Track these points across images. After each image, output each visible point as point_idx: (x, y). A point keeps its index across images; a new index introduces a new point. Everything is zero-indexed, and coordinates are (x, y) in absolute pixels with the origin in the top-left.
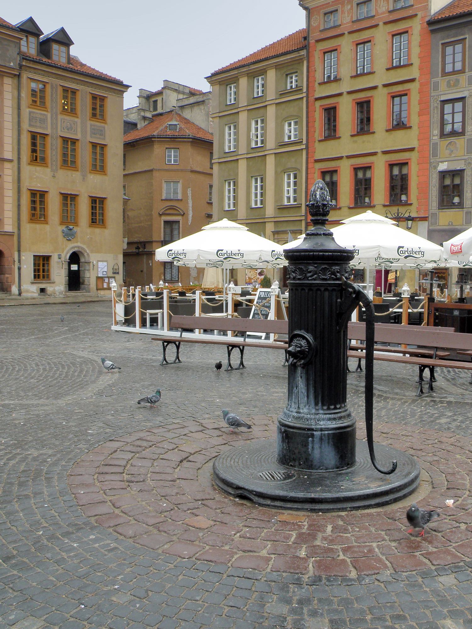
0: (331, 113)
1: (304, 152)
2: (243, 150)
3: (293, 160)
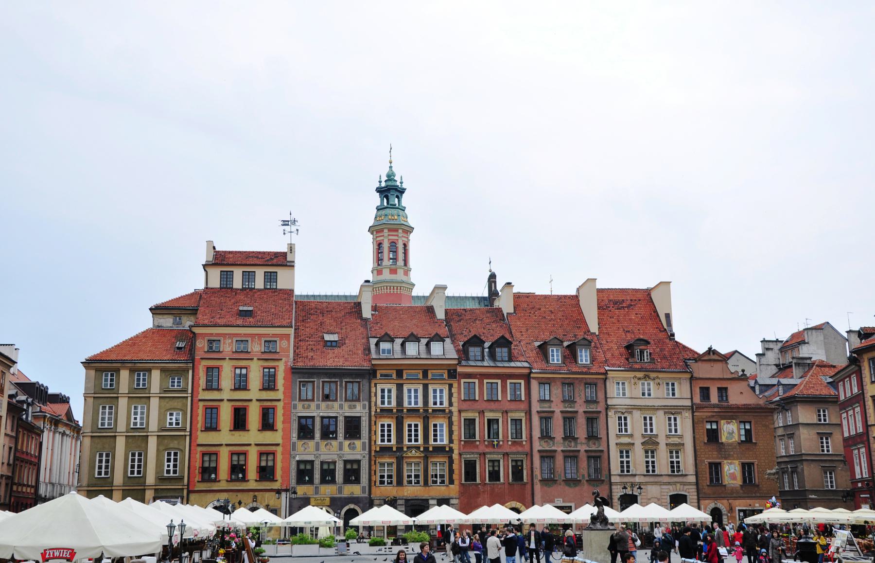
0: (212, 411)
1: (188, 438)
3: (176, 442)
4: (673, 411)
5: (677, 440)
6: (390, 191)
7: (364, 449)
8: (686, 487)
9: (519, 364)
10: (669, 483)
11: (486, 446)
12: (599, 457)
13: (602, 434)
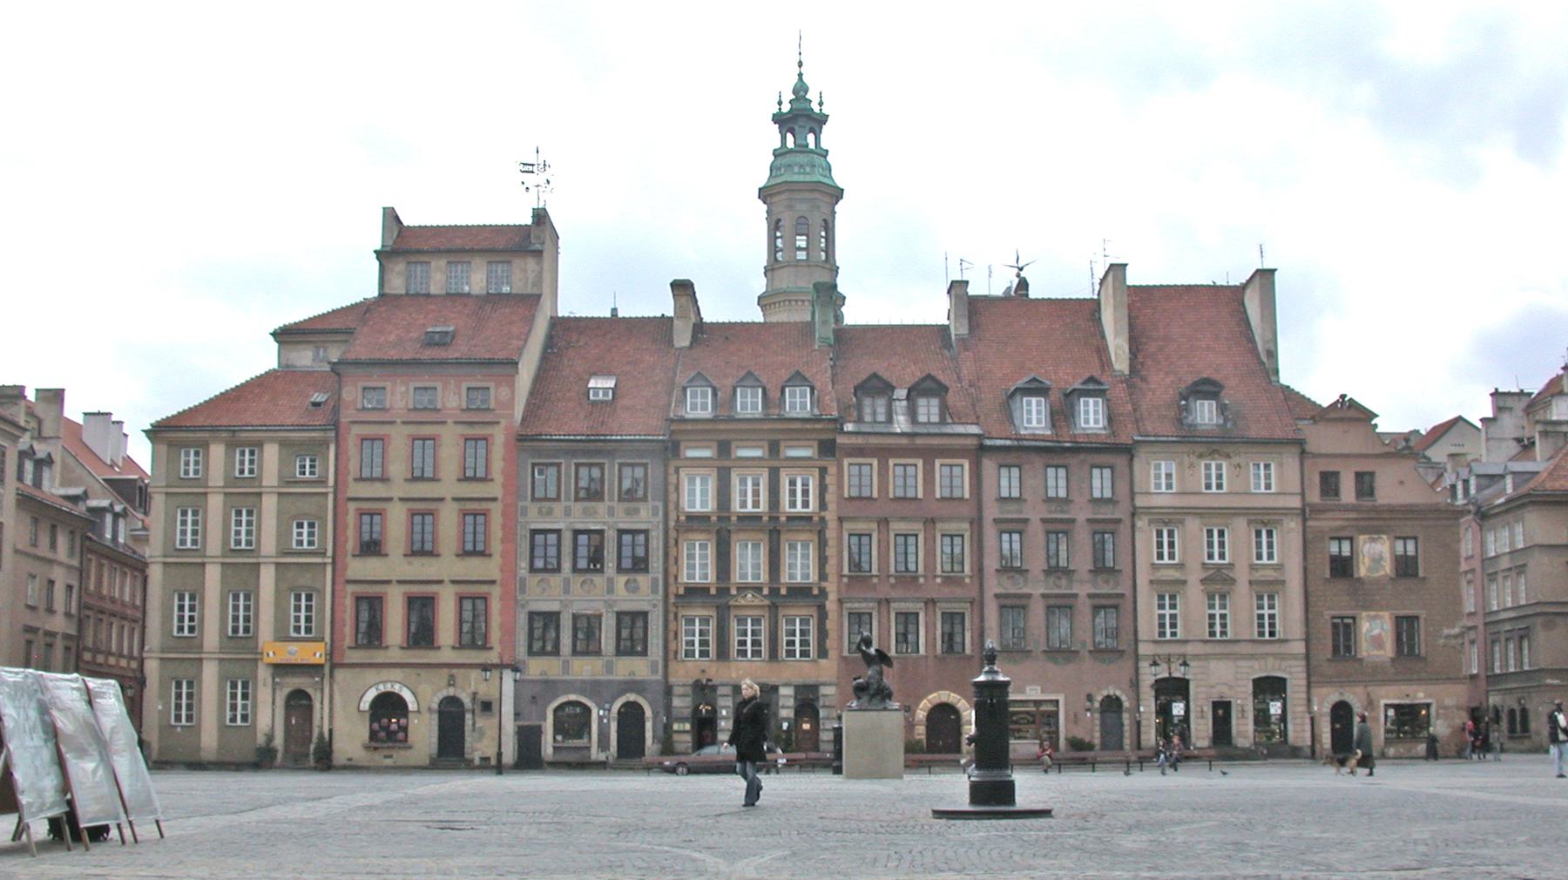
1: (329, 569)
2: (214, 546)
4: (1266, 518)
5: (1271, 575)
6: (800, 118)
7: (654, 591)
8: (1285, 664)
9: (960, 429)
10: (1252, 657)
11: (893, 586)
12: (1116, 607)
13: (1124, 564)
